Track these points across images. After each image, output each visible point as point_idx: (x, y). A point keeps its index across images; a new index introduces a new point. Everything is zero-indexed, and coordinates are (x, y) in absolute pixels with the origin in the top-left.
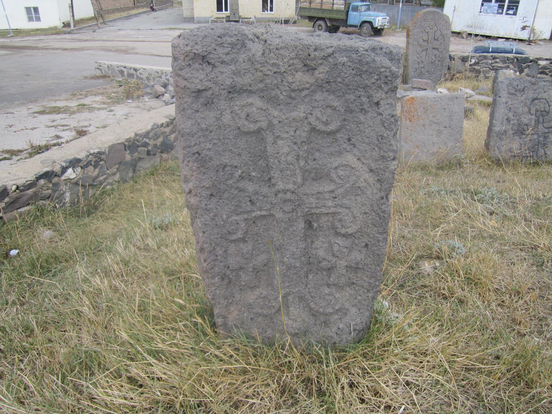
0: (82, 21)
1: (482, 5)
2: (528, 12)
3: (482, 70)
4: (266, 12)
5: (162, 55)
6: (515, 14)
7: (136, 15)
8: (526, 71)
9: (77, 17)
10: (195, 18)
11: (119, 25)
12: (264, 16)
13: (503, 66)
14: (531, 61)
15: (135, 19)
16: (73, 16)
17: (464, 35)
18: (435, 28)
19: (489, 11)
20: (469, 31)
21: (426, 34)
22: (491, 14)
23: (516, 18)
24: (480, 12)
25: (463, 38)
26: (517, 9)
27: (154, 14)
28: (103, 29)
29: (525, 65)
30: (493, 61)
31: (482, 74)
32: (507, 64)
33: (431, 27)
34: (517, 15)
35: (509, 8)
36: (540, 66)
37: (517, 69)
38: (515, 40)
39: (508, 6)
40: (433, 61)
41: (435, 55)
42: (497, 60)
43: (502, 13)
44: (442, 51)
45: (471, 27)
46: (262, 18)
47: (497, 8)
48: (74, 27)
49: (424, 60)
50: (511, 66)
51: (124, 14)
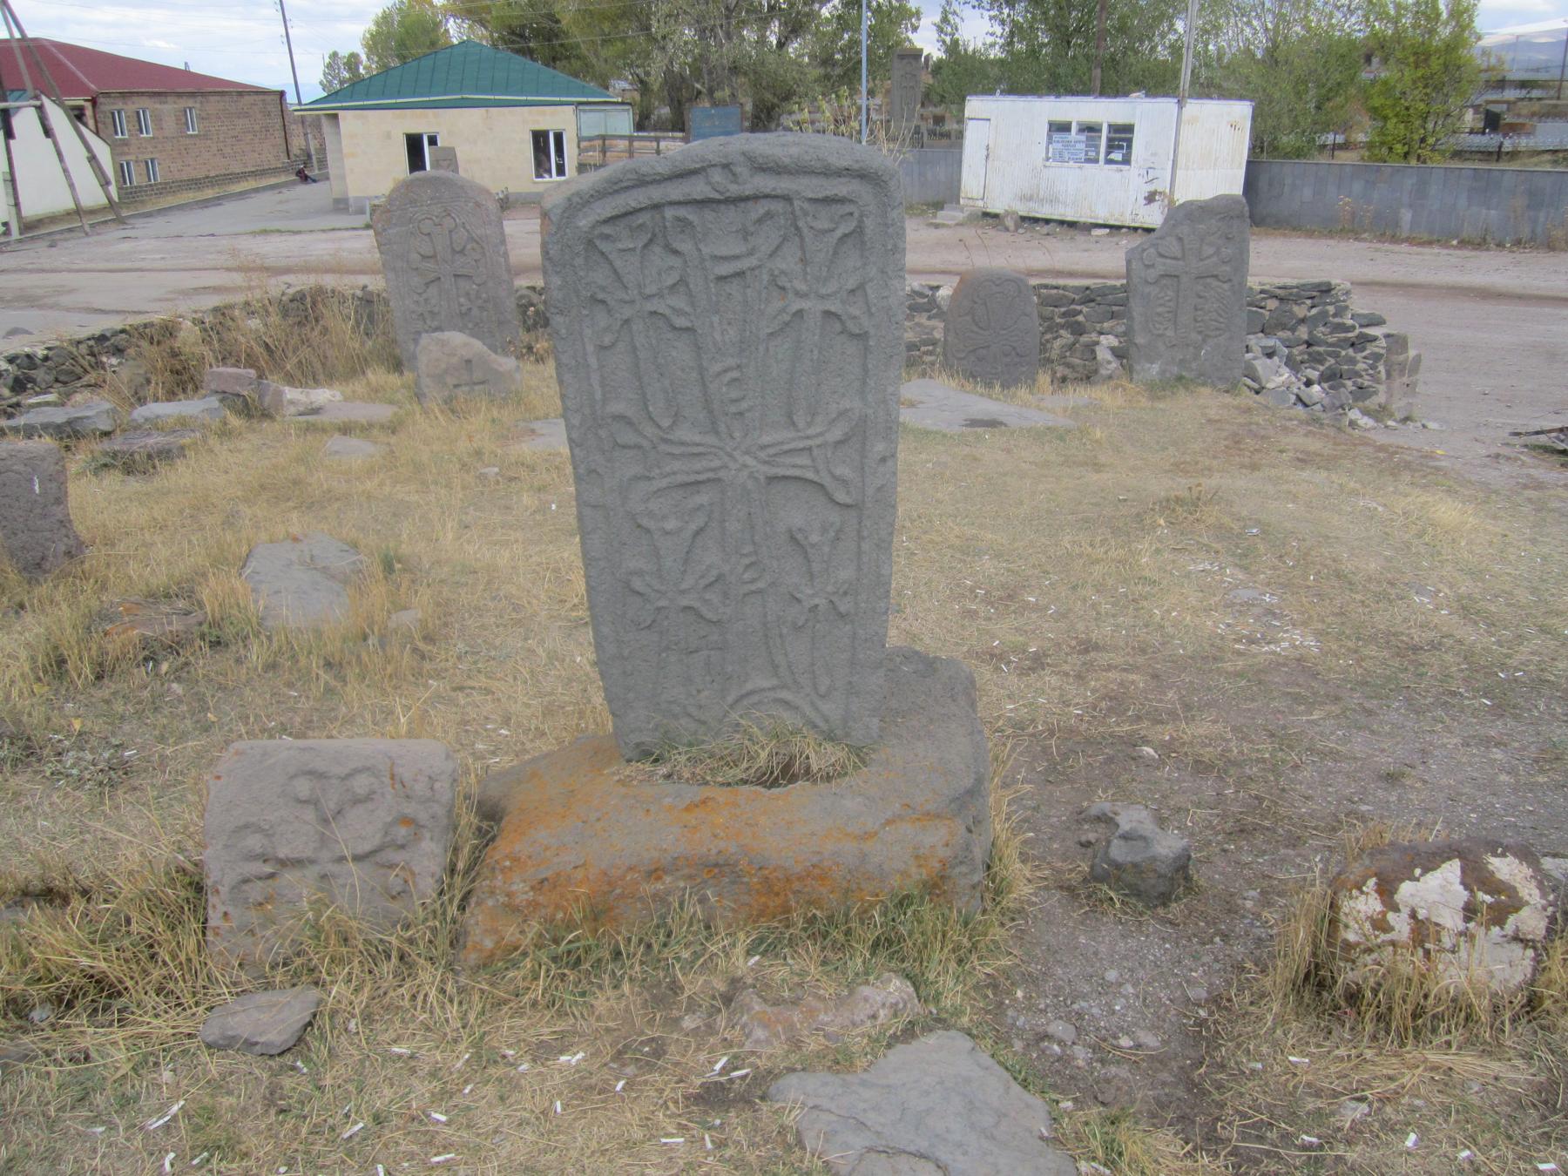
0: (52, 219)
1: (1050, 138)
2: (1154, 154)
4: (547, 179)
5: (108, 308)
6: (1126, 161)
7: (242, 195)
9: (31, 209)
10: (351, 201)
11: (179, 222)
15: (229, 206)
16: (17, 205)
17: (1010, 223)
18: (448, 222)
19: (1066, 156)
20: (1023, 211)
21: (426, 238)
22: (1071, 163)
23: (1133, 172)
24: (1048, 159)
25: (1007, 229)
26: (1129, 147)
27: (303, 190)
28: (95, 238)
33: (437, 220)
34: (1133, 163)
35: (1111, 148)
38: (1136, 229)
39: (1110, 140)
40: (464, 309)
41: (468, 294)
43: (1096, 161)
44: (485, 283)
45: (1030, 199)
47: (1082, 146)
48: (21, 234)
49: (436, 310)
51: (209, 193)
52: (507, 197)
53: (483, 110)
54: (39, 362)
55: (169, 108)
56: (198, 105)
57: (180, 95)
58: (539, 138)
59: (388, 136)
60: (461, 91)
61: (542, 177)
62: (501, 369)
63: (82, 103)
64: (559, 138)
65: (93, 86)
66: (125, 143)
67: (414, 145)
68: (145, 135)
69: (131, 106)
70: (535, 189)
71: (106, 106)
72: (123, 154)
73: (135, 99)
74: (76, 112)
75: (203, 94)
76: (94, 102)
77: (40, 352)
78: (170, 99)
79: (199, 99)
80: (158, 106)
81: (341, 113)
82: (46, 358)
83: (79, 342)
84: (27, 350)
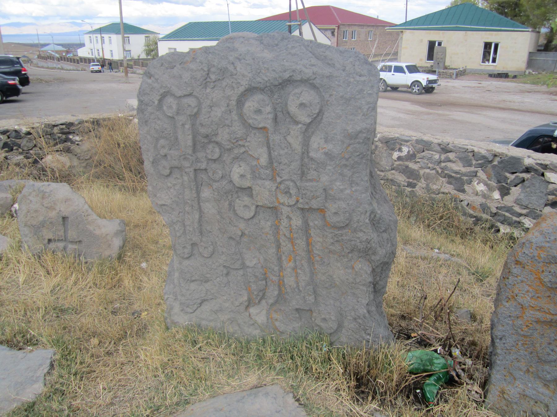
3: (422, 172)
4: (487, 63)
8: (515, 191)
12: (483, 68)
13: (464, 170)
14: (528, 170)
29: (513, 177)
30: (443, 157)
31: (422, 180)
32: (473, 169)
36: (551, 187)
37: (493, 184)
42: (451, 156)
46: (481, 70)
50: (481, 174)
52: (465, 70)
53: (464, 32)
54: (23, 135)
55: (365, 30)
56: (374, 30)
57: (368, 26)
58: (487, 46)
59: (421, 41)
60: (457, 24)
61: (484, 62)
62: (97, 232)
63: (335, 27)
64: (496, 46)
65: (340, 22)
66: (346, 42)
67: (432, 45)
68: (353, 39)
69: (350, 30)
70: (480, 68)
71: (343, 29)
72: (345, 46)
73: (353, 27)
74: (332, 31)
75: (377, 26)
76: (339, 27)
77: (24, 129)
78: (365, 27)
79: (375, 28)
80: (360, 30)
81: (404, 30)
82: (29, 133)
83: (54, 126)
84: (16, 127)
